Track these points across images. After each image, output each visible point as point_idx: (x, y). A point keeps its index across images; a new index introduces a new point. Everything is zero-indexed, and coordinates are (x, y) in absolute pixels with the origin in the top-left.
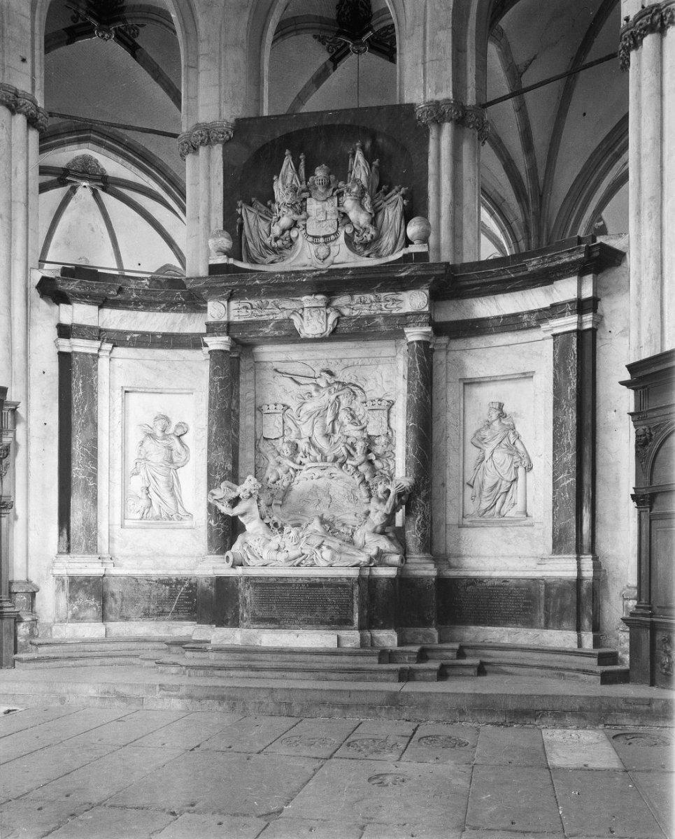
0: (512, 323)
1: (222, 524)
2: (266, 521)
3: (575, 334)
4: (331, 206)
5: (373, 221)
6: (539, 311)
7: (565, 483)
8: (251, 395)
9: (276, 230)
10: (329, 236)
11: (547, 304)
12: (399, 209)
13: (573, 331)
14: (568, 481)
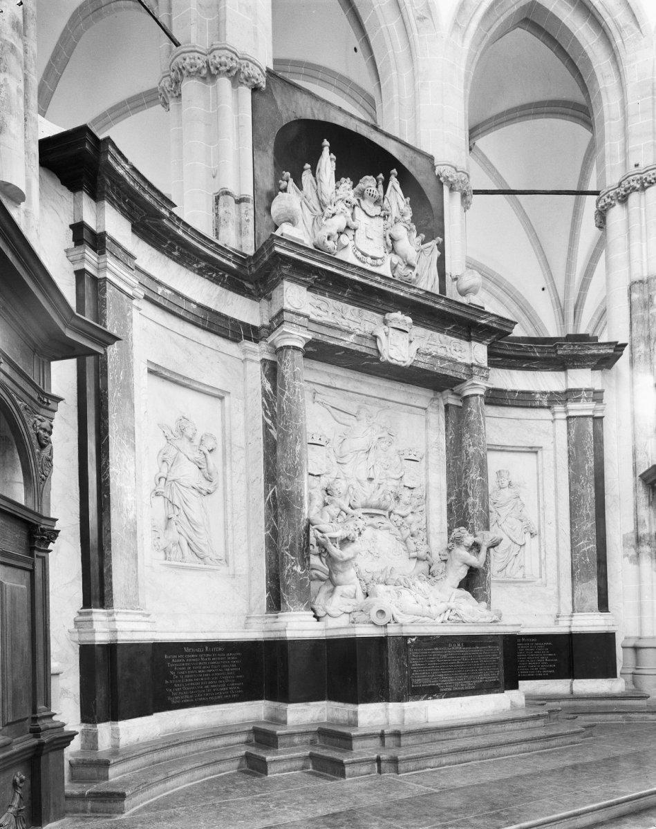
6: (551, 393)
7: (585, 549)
14: (588, 547)
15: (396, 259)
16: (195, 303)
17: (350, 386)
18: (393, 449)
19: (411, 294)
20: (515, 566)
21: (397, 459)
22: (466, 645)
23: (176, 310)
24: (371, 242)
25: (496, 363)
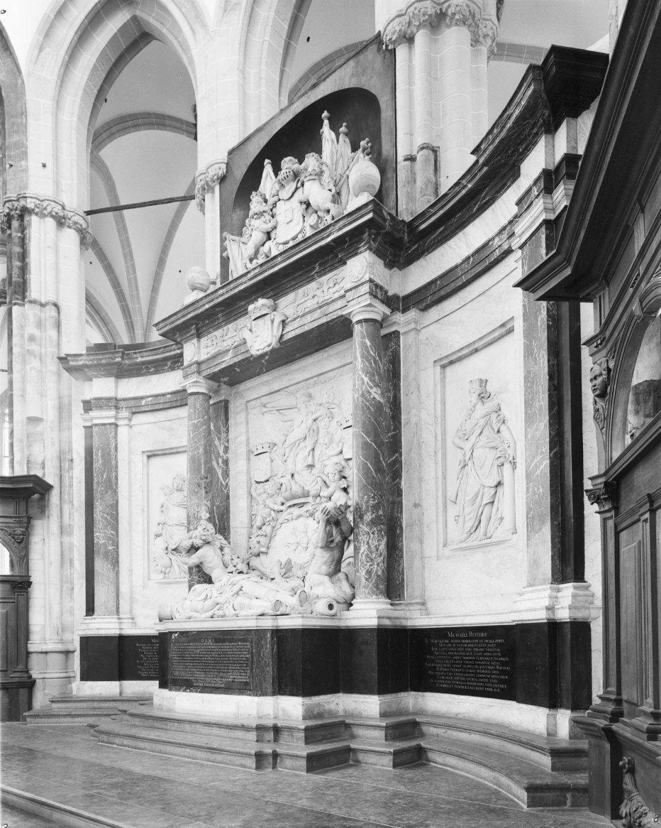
17: (285, 382)
18: (334, 423)
22: (217, 641)
23: (157, 407)
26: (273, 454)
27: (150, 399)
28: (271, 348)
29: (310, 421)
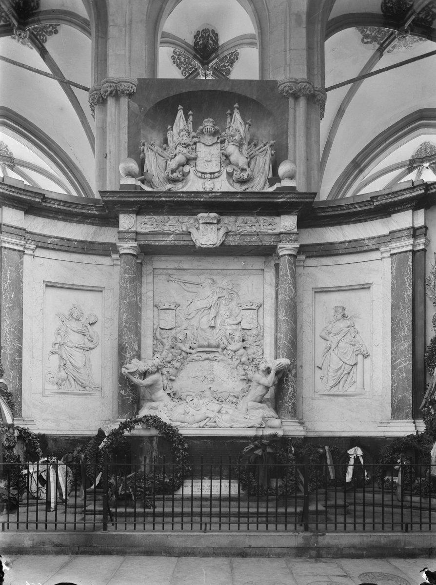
0: (355, 248)
1: (131, 394)
2: (169, 391)
3: (411, 253)
4: (216, 150)
5: (249, 164)
6: (378, 237)
7: (402, 366)
8: (150, 294)
9: (173, 164)
10: (214, 173)
11: (386, 232)
12: (268, 157)
13: (409, 251)
14: (404, 365)
15: (230, 169)
16: (76, 241)
18: (234, 303)
19: (210, 198)
20: (348, 382)
21: (237, 311)
24: (210, 163)
25: (326, 223)
26: (177, 312)
27: (56, 240)
28: (214, 246)
29: (215, 298)
